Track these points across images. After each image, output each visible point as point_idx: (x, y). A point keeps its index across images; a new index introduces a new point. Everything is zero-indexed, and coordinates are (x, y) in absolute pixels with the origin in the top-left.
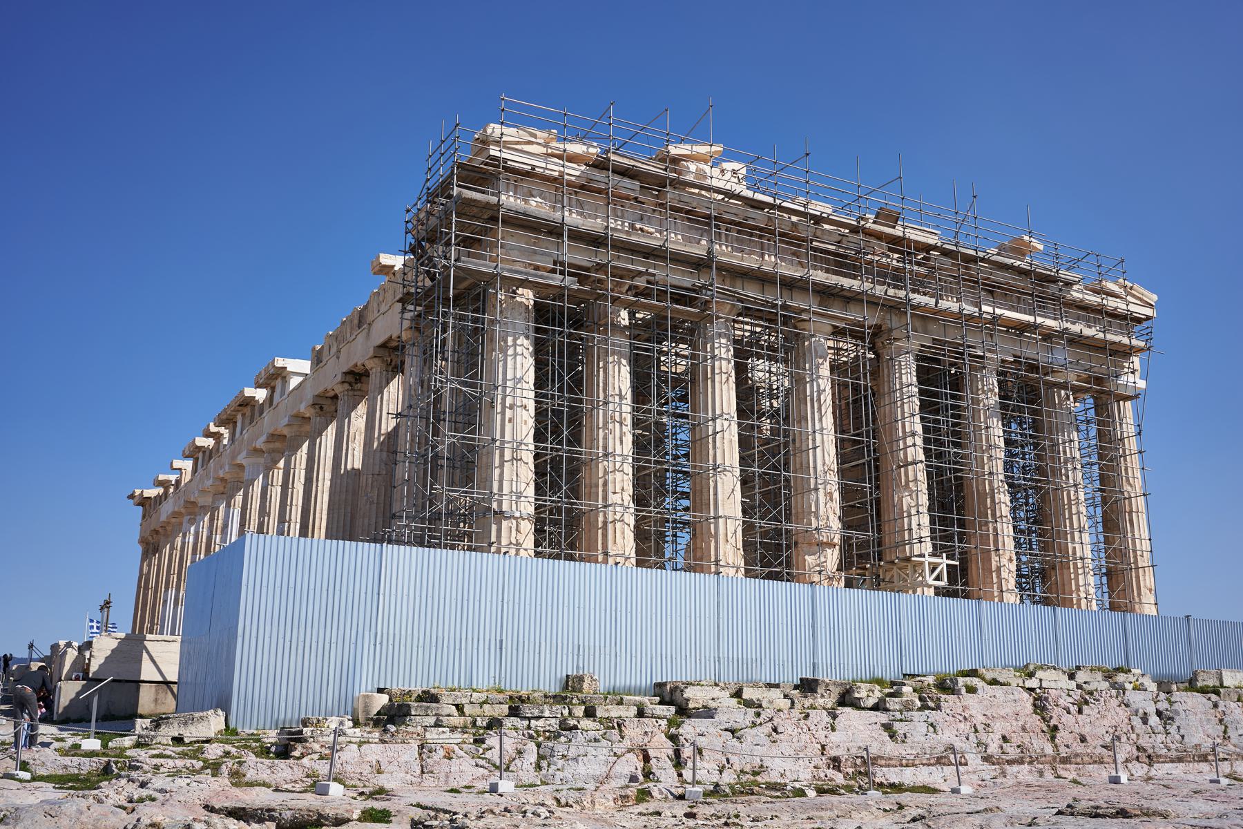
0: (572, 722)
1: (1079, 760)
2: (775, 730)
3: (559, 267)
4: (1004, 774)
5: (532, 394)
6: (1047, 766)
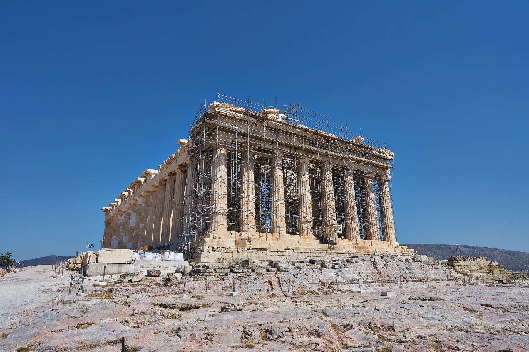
0: (249, 274)
3: (234, 143)
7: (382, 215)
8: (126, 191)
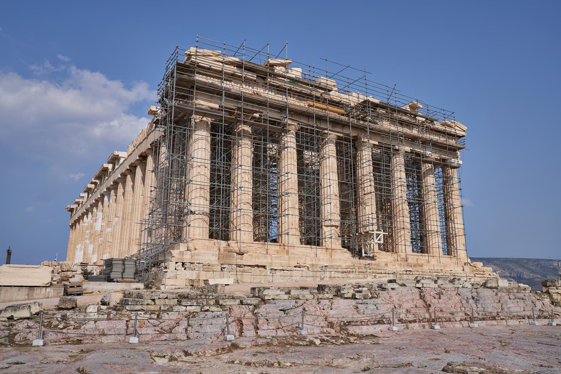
1: (440, 320)
2: (304, 309)
4: (407, 327)
5: (209, 162)
6: (426, 323)
7: (447, 218)
8: (92, 183)
